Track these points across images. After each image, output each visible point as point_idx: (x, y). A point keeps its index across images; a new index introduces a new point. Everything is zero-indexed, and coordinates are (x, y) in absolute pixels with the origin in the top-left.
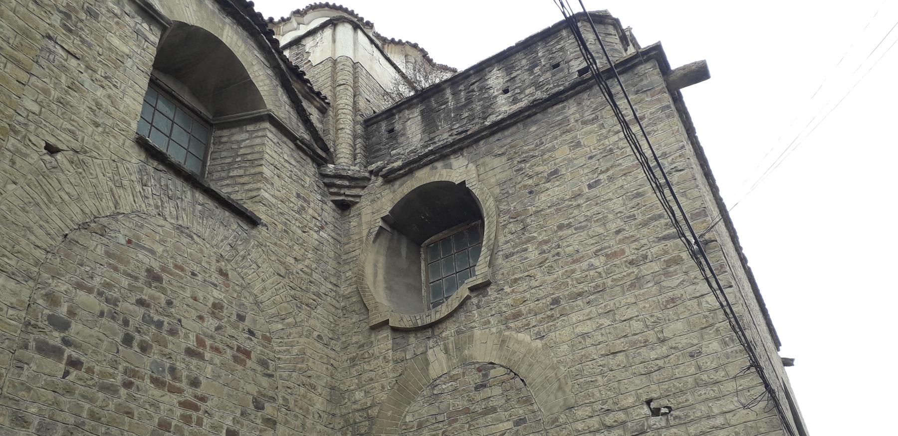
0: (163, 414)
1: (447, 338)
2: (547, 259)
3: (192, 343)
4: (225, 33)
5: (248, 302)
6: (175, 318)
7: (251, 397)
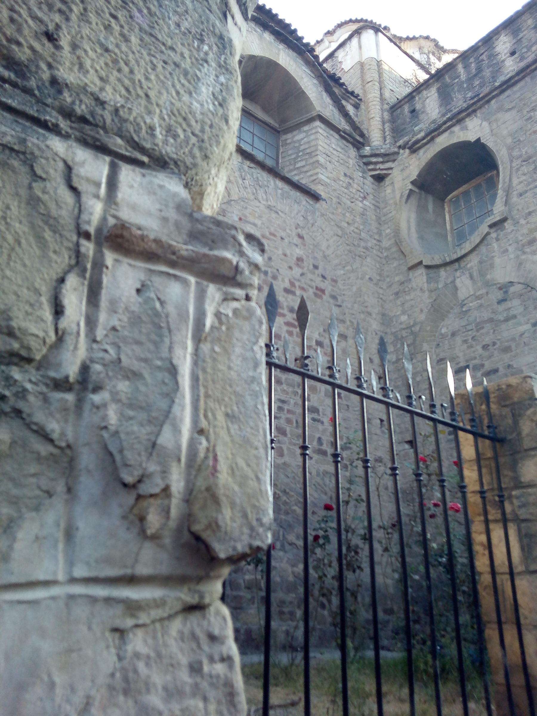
1: (472, 268)
3: (287, 285)
5: (319, 255)
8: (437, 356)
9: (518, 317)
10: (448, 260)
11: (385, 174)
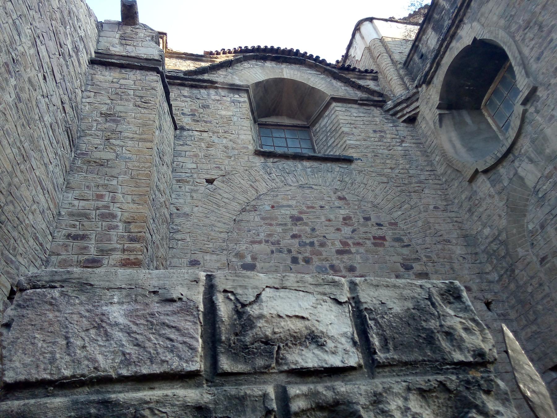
1: (527, 151)
4: (285, 73)
5: (367, 207)
6: (321, 236)
7: (399, 264)
8: (537, 256)
10: (500, 155)
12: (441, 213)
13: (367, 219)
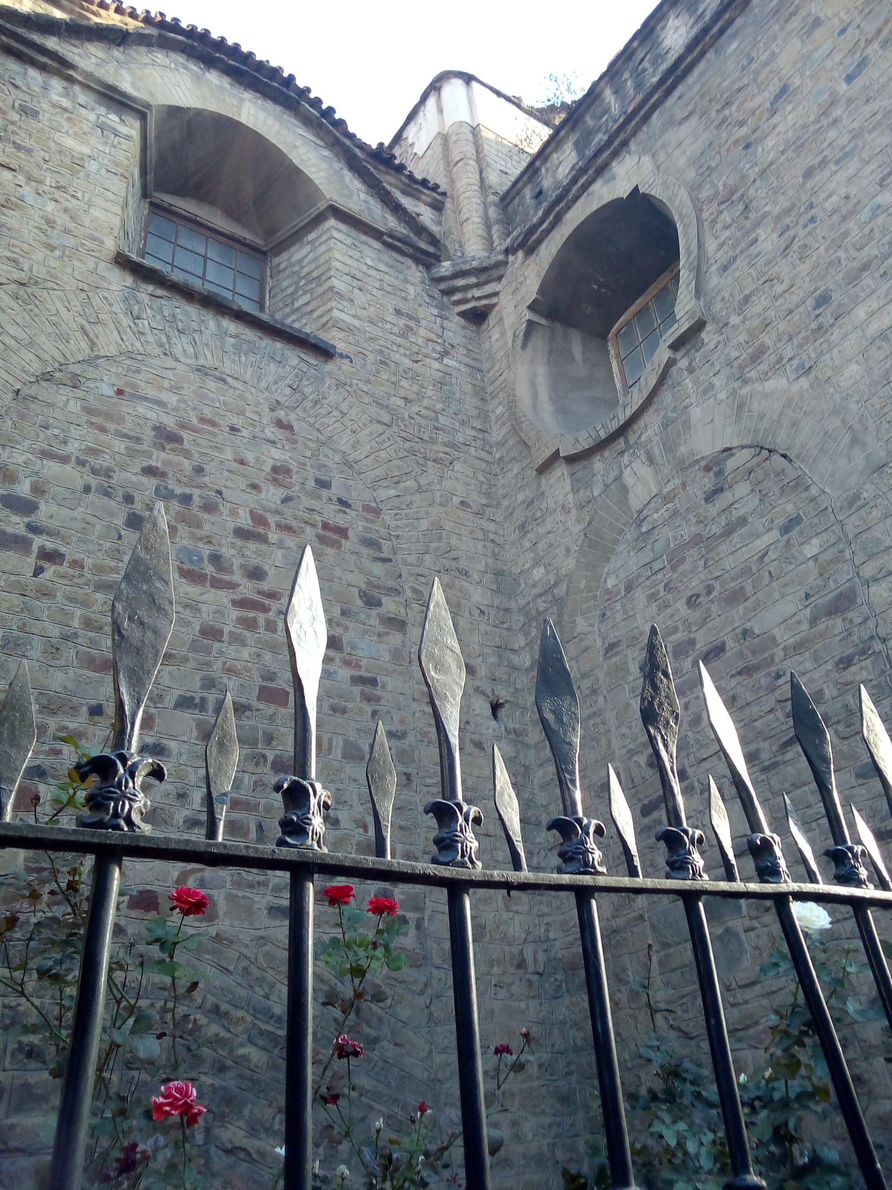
0: (207, 615)
2: (794, 237)
4: (244, 111)
5: (332, 460)
6: (211, 489)
7: (356, 591)
9: (750, 520)
10: (603, 435)
11: (485, 306)
12: (470, 516)
13: (324, 484)
